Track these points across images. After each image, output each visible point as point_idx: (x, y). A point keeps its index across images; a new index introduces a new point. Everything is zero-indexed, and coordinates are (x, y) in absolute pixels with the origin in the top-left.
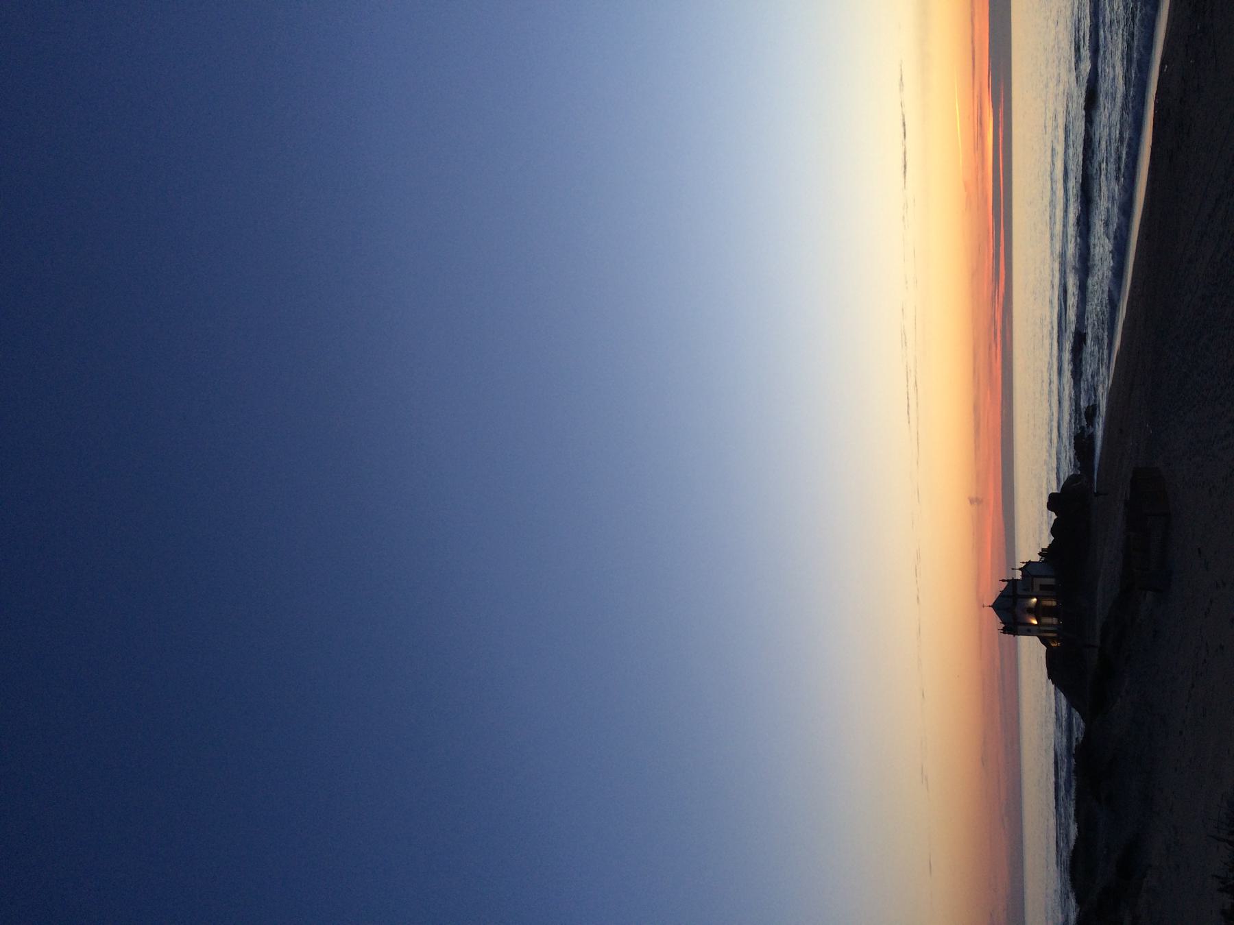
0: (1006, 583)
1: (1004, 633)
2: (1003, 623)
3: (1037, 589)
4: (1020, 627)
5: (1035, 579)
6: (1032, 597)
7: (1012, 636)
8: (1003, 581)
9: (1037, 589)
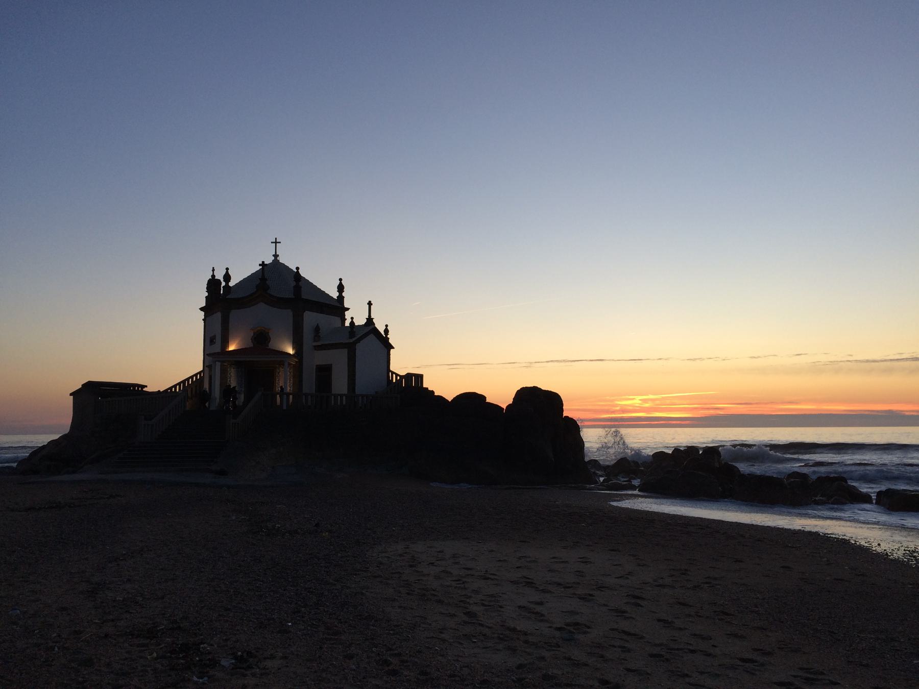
1: (213, 284)
3: (322, 358)
4: (218, 316)
5: (345, 351)
6: (297, 345)
7: (203, 304)
8: (341, 288)
9: (322, 358)
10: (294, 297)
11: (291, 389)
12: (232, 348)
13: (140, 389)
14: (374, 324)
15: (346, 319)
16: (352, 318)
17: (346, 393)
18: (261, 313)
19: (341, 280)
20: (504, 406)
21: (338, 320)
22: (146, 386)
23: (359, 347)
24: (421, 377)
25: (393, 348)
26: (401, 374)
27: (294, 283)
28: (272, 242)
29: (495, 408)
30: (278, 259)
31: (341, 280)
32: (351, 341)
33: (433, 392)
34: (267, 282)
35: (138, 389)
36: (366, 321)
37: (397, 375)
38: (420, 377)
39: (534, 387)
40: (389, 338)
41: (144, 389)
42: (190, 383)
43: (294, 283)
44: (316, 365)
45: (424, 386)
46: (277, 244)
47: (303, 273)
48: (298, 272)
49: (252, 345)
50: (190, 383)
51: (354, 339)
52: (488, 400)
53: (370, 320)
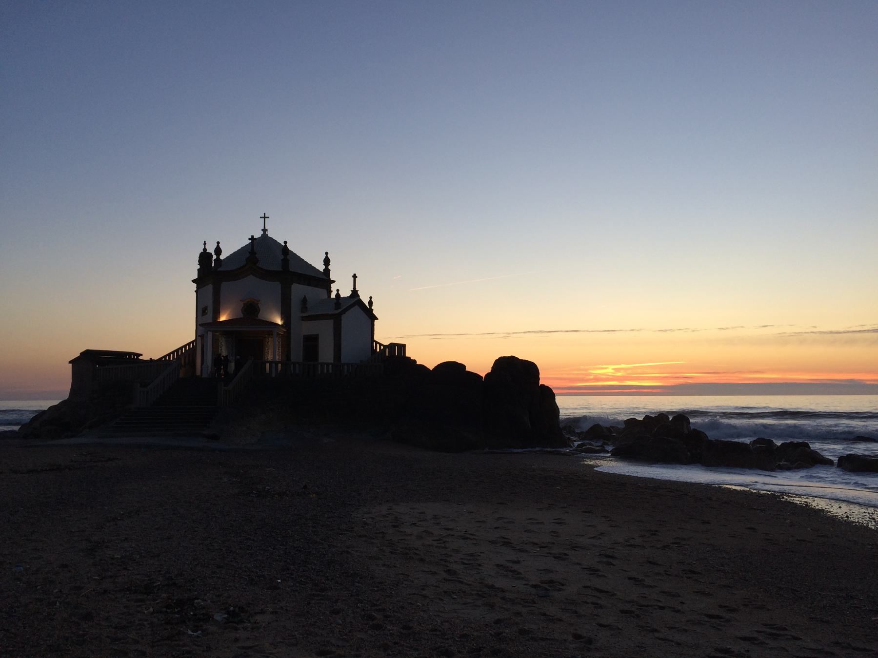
0: (321, 267)
1: (204, 257)
4: (210, 288)
5: (330, 323)
6: (286, 316)
7: (196, 277)
8: (327, 261)
10: (282, 270)
11: (280, 358)
12: (223, 318)
13: (136, 357)
14: (359, 296)
15: (332, 291)
16: (338, 290)
17: (332, 362)
18: (251, 285)
19: (327, 253)
20: (483, 375)
21: (322, 292)
22: (142, 355)
23: (344, 317)
24: (405, 345)
25: (377, 319)
26: (385, 344)
27: (282, 257)
28: (261, 218)
29: (475, 376)
30: (267, 233)
31: (327, 253)
32: (337, 312)
33: (415, 361)
34: (256, 255)
35: (134, 357)
36: (351, 293)
37: (381, 345)
38: (402, 347)
39: (512, 356)
40: (373, 310)
41: (139, 358)
42: (183, 352)
43: (282, 257)
44: (304, 335)
45: (407, 355)
46: (266, 219)
47: (290, 247)
48: (286, 246)
49: (242, 316)
50: (183, 352)
51: (340, 310)
52: (467, 369)
53: (355, 293)
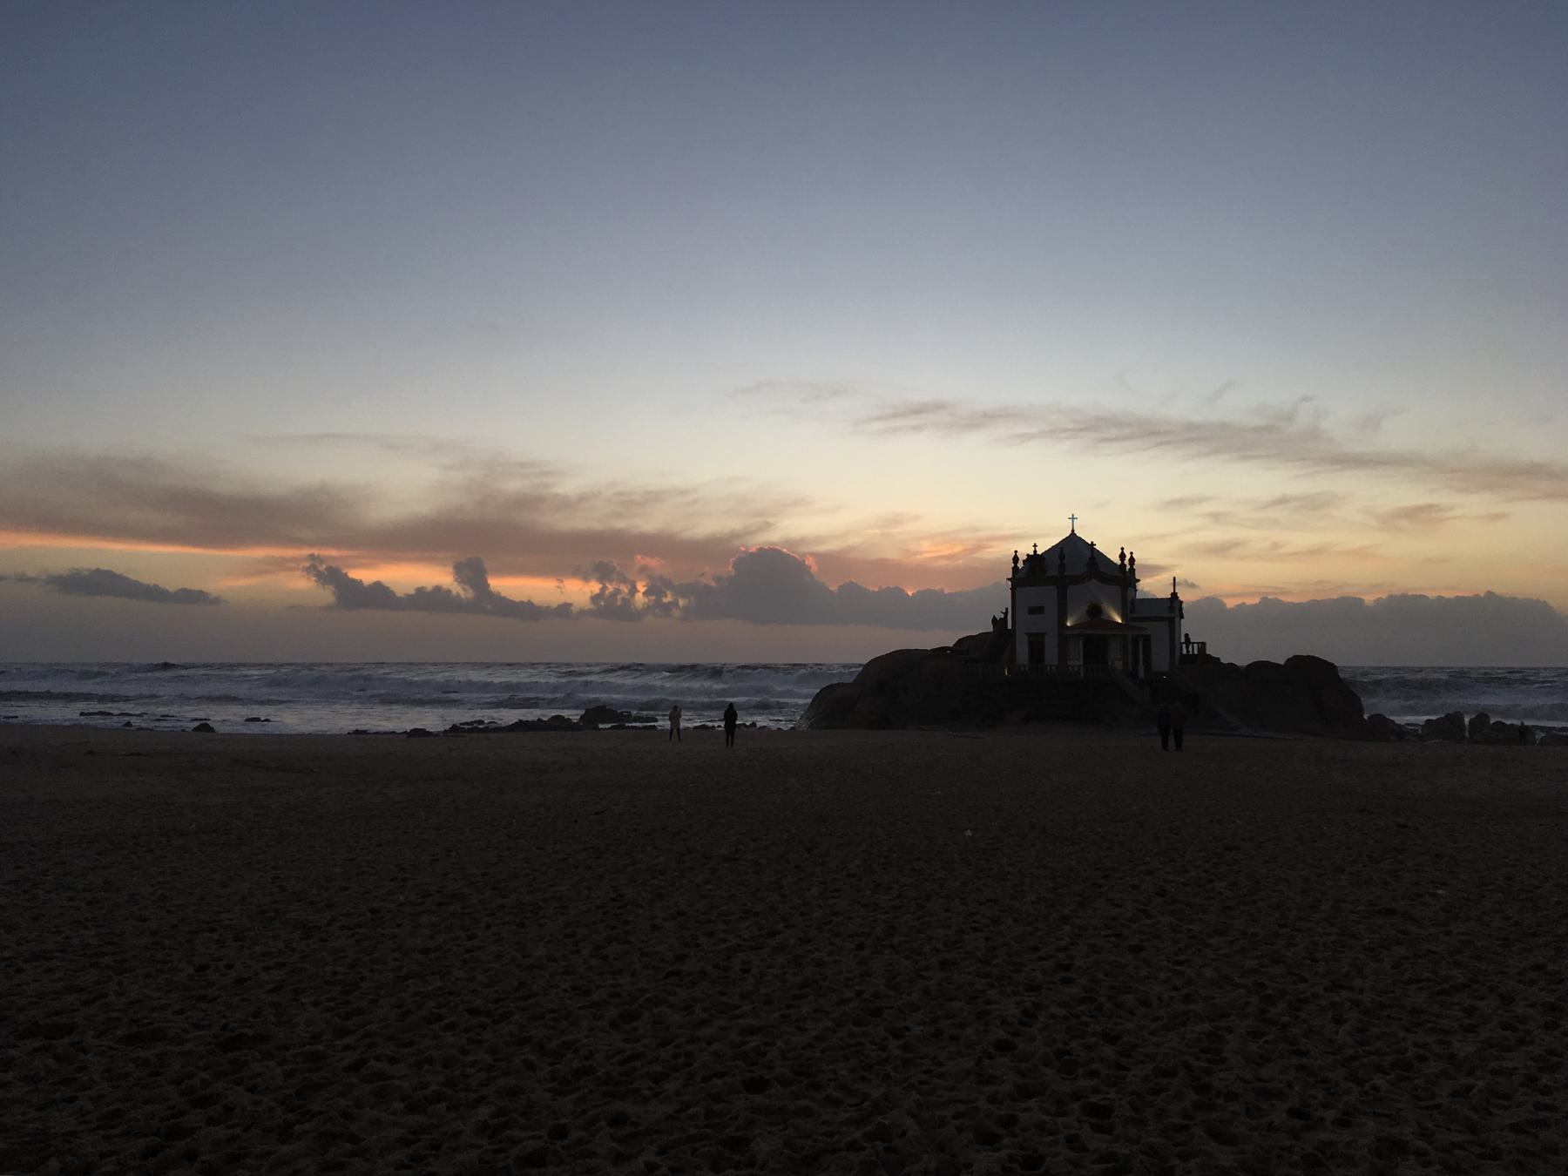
2: (1062, 557)
8: (1132, 560)
24: (1204, 644)
45: (1208, 652)
53: (1174, 595)
